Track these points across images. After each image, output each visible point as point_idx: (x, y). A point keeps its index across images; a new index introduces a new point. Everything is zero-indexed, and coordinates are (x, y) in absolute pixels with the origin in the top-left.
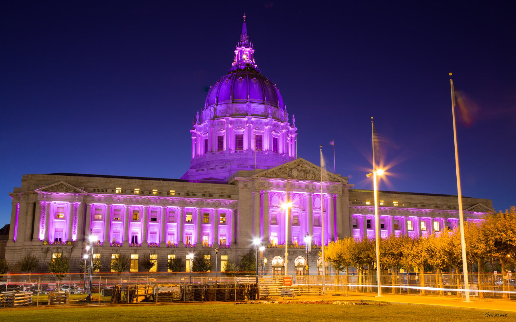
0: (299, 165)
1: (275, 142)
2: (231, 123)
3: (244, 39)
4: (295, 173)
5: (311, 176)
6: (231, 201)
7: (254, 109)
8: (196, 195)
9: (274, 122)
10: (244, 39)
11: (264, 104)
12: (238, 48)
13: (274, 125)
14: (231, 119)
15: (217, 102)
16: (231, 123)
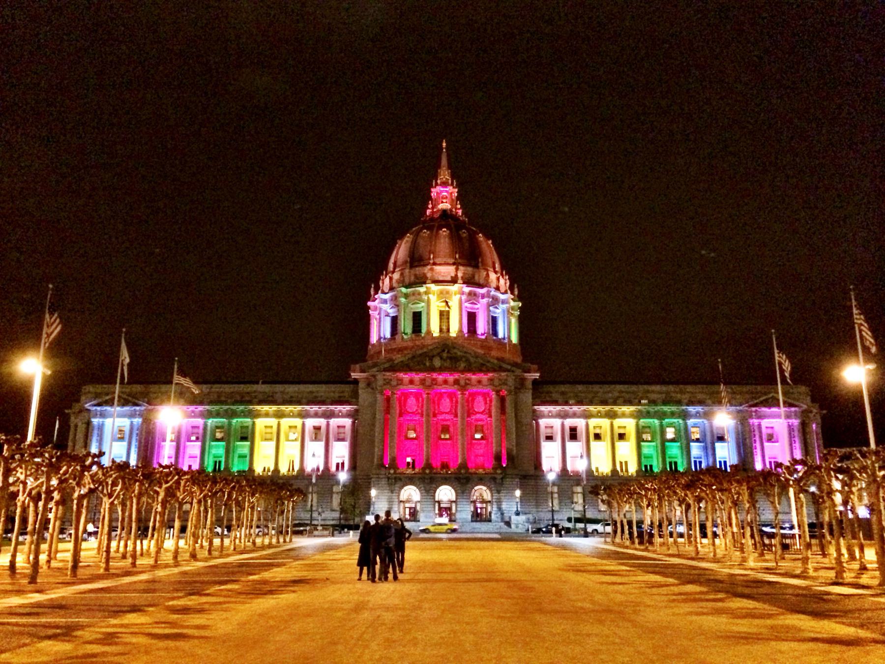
0: (444, 351)
1: (472, 318)
2: (406, 296)
3: (444, 174)
4: (437, 363)
5: (463, 365)
6: (348, 408)
7: (439, 273)
8: (299, 403)
9: (467, 289)
10: (444, 174)
11: (454, 264)
12: (433, 190)
13: (470, 294)
14: (404, 290)
15: (395, 268)
16: (406, 296)
